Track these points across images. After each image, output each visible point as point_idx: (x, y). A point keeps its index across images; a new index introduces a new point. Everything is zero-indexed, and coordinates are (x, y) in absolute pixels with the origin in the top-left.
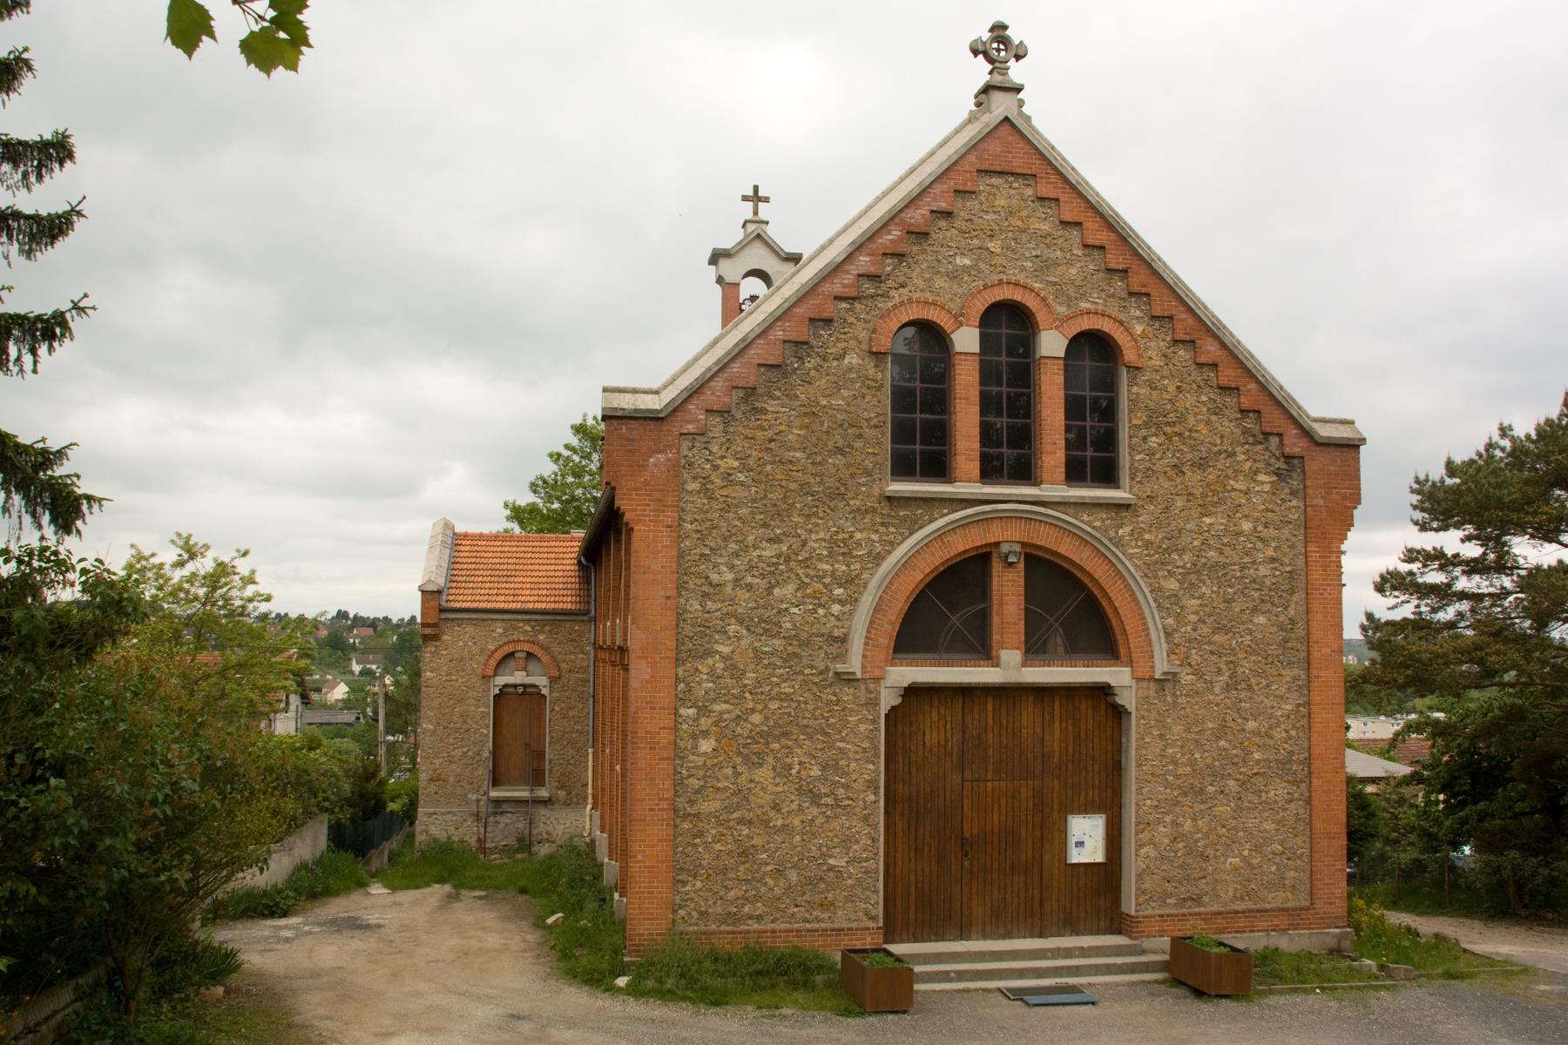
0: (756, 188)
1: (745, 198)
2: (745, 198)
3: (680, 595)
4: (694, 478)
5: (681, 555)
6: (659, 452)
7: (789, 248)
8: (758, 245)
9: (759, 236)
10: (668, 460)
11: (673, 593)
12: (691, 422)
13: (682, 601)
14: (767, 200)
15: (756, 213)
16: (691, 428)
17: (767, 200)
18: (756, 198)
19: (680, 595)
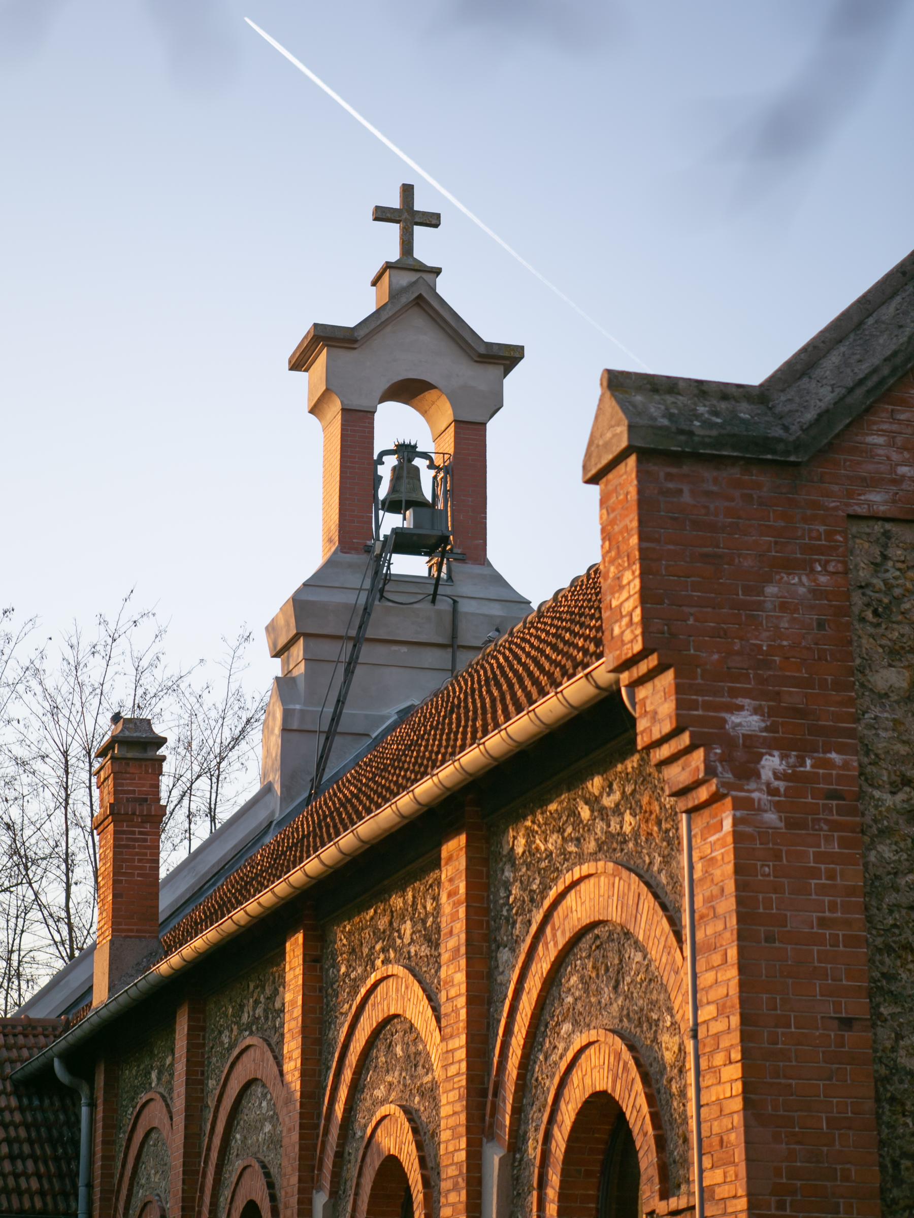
0: (407, 191)
1: (382, 215)
2: (382, 215)
3: (877, 1018)
4: (895, 653)
5: (874, 886)
6: (790, 566)
7: (490, 330)
8: (417, 320)
9: (420, 297)
10: (817, 592)
11: (857, 1007)
12: (873, 482)
13: (885, 1035)
14: (432, 220)
15: (407, 245)
16: (877, 499)
17: (432, 220)
18: (407, 215)
19: (877, 1018)
